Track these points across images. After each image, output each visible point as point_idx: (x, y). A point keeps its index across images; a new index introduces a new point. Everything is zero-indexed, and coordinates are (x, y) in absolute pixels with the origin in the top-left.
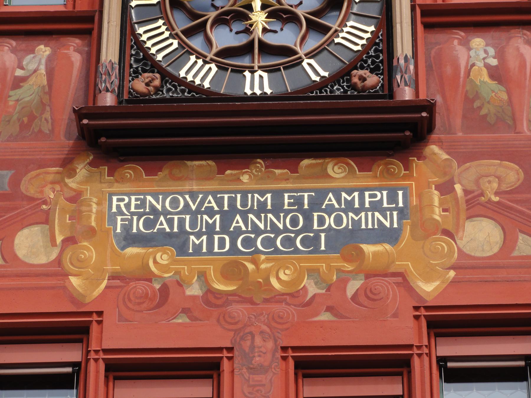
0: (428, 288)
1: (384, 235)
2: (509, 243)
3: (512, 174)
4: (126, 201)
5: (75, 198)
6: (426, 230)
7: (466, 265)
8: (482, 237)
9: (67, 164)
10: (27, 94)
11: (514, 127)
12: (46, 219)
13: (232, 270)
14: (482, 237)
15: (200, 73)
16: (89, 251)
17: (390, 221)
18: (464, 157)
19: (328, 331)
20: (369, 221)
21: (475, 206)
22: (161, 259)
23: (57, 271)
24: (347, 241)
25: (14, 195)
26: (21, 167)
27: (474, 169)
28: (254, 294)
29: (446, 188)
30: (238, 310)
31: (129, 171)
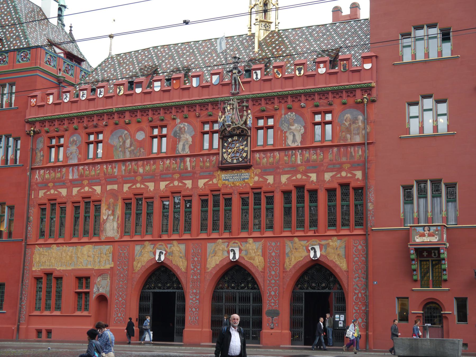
0: (251, 185)
1: (247, 179)
2: (259, 179)
3: (260, 171)
4: (224, 175)
5: (219, 175)
6: (251, 178)
7: (255, 182)
8: (256, 178)
9: (218, 171)
10: (214, 162)
11: (260, 164)
12: (216, 178)
13: (233, 183)
14: (256, 178)
15: (230, 161)
16: (220, 181)
17: (248, 177)
18: (255, 169)
19: (242, 190)
20: (246, 177)
21: (256, 175)
22: (227, 182)
23: (217, 184)
24: (244, 179)
25: (213, 175)
26: (213, 171)
27: (256, 170)
28: (235, 186)
29: (253, 173)
30: (234, 188)
31: (224, 172)
